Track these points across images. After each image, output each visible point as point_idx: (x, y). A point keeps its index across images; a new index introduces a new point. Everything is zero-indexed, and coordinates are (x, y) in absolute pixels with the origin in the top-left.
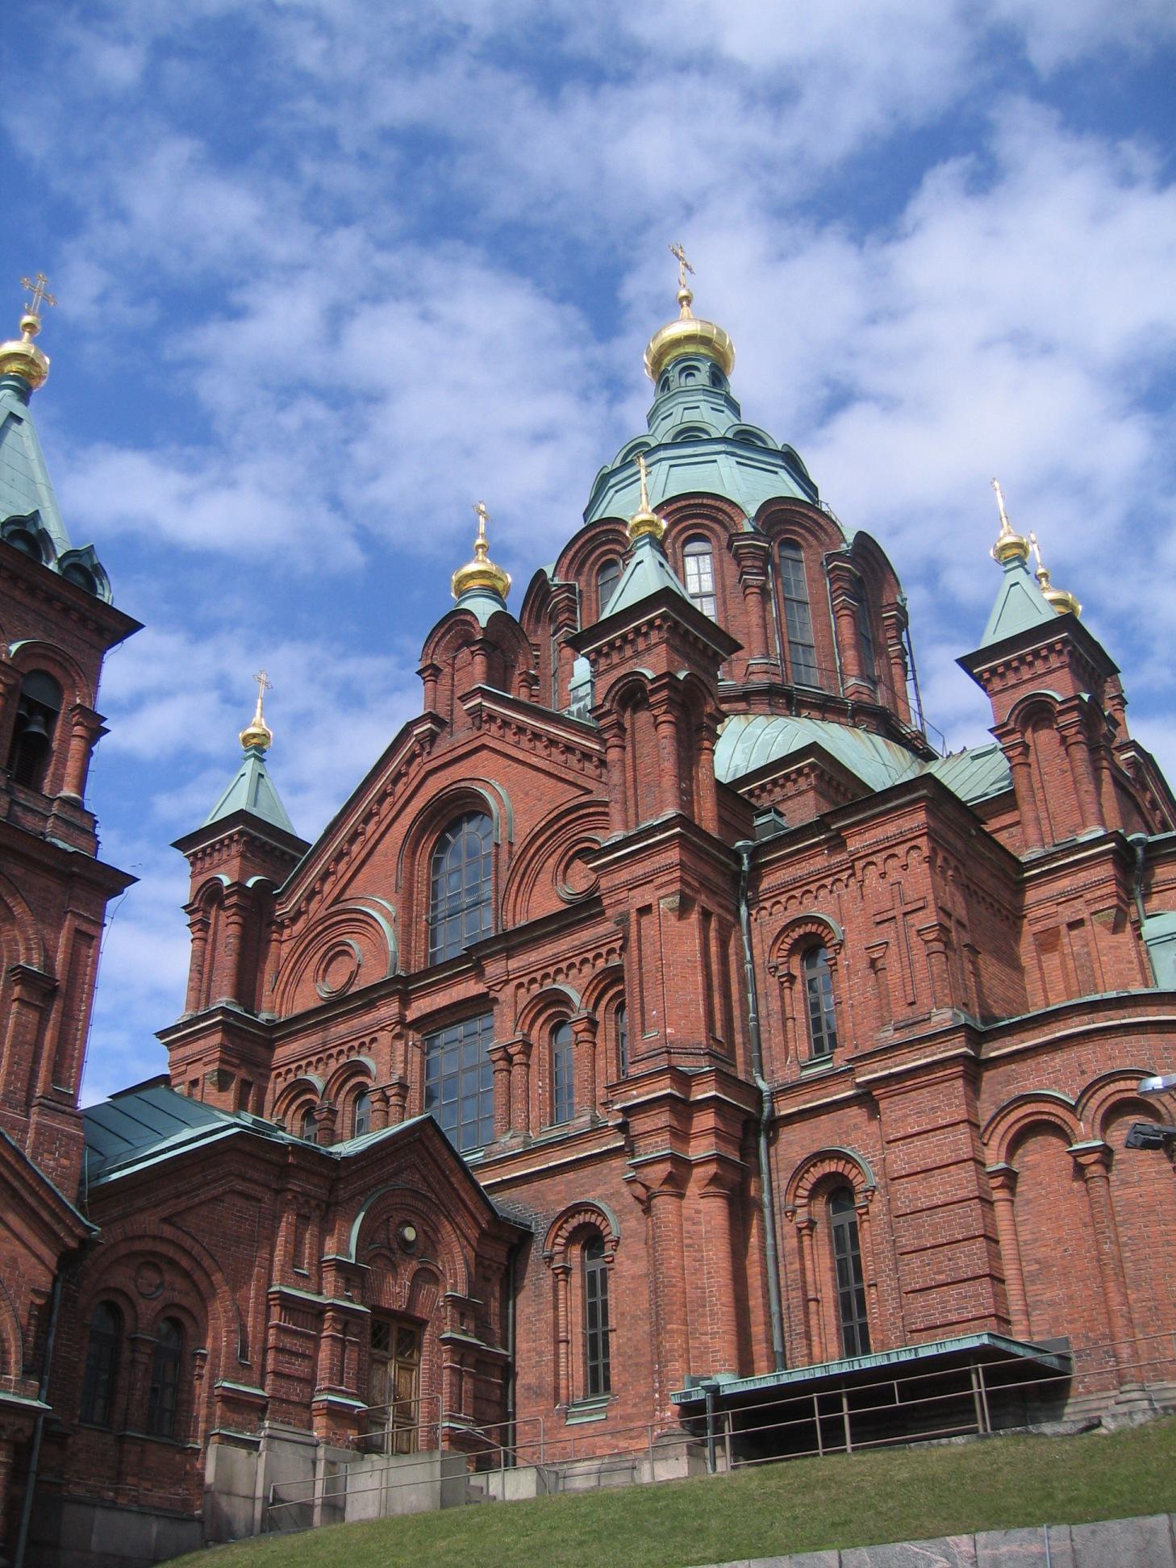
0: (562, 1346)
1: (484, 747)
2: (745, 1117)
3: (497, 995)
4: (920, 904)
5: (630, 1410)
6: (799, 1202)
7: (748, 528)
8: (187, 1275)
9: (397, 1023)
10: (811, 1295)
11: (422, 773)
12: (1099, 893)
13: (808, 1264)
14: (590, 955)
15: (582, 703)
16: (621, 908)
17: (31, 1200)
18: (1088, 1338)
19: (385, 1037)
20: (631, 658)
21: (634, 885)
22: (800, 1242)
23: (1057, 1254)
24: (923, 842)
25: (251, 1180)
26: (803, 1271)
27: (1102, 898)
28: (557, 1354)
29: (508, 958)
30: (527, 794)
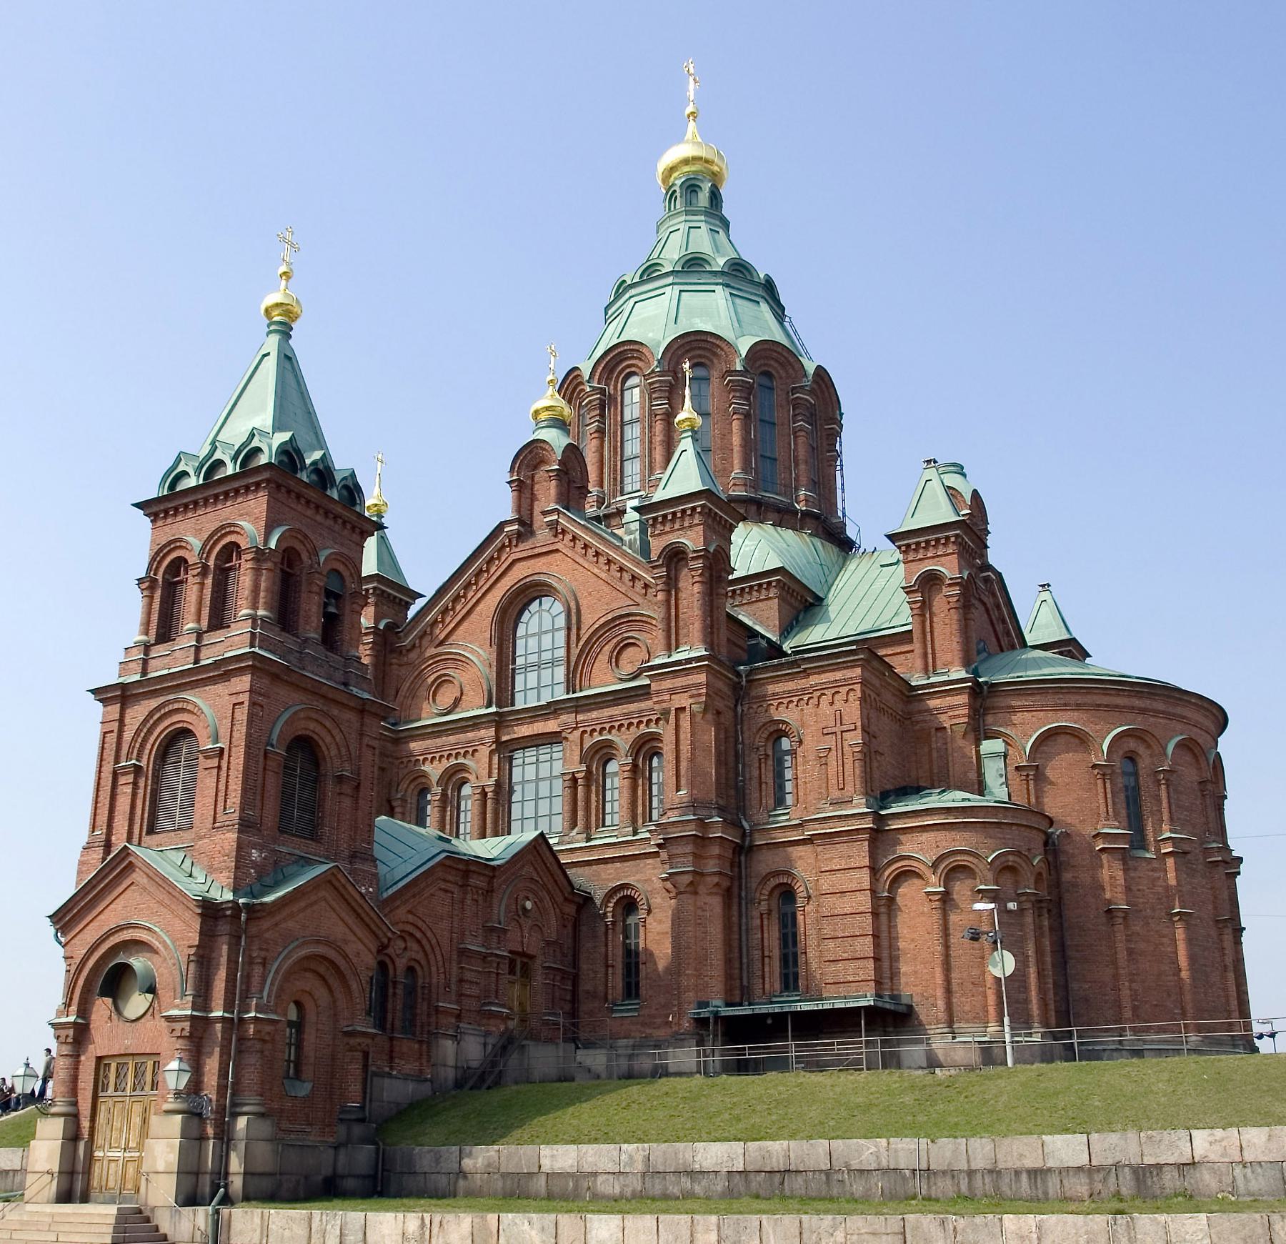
0: (610, 969)
1: (557, 551)
2: (734, 845)
3: (568, 736)
4: (852, 727)
5: (653, 1012)
6: (763, 897)
7: (739, 367)
8: (419, 942)
9: (493, 742)
10: (766, 953)
11: (510, 560)
12: (957, 713)
13: (766, 935)
14: (635, 721)
15: (632, 537)
16: (664, 705)
17: (367, 919)
18: (923, 996)
19: (484, 751)
20: (678, 530)
21: (673, 691)
22: (762, 921)
23: (912, 946)
24: (858, 687)
25: (448, 881)
26: (762, 938)
27: (959, 716)
28: (607, 974)
29: (577, 713)
30: (590, 594)
